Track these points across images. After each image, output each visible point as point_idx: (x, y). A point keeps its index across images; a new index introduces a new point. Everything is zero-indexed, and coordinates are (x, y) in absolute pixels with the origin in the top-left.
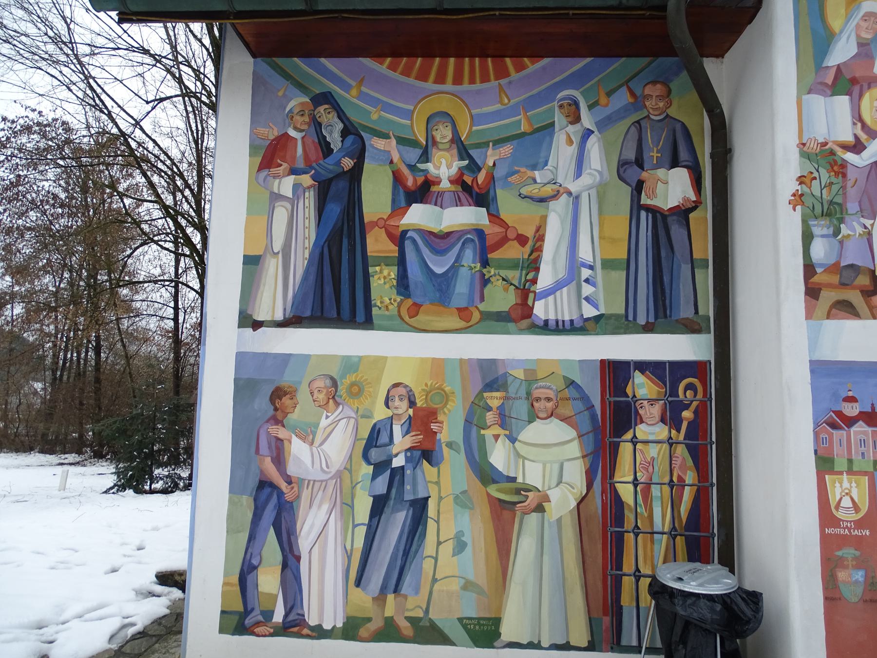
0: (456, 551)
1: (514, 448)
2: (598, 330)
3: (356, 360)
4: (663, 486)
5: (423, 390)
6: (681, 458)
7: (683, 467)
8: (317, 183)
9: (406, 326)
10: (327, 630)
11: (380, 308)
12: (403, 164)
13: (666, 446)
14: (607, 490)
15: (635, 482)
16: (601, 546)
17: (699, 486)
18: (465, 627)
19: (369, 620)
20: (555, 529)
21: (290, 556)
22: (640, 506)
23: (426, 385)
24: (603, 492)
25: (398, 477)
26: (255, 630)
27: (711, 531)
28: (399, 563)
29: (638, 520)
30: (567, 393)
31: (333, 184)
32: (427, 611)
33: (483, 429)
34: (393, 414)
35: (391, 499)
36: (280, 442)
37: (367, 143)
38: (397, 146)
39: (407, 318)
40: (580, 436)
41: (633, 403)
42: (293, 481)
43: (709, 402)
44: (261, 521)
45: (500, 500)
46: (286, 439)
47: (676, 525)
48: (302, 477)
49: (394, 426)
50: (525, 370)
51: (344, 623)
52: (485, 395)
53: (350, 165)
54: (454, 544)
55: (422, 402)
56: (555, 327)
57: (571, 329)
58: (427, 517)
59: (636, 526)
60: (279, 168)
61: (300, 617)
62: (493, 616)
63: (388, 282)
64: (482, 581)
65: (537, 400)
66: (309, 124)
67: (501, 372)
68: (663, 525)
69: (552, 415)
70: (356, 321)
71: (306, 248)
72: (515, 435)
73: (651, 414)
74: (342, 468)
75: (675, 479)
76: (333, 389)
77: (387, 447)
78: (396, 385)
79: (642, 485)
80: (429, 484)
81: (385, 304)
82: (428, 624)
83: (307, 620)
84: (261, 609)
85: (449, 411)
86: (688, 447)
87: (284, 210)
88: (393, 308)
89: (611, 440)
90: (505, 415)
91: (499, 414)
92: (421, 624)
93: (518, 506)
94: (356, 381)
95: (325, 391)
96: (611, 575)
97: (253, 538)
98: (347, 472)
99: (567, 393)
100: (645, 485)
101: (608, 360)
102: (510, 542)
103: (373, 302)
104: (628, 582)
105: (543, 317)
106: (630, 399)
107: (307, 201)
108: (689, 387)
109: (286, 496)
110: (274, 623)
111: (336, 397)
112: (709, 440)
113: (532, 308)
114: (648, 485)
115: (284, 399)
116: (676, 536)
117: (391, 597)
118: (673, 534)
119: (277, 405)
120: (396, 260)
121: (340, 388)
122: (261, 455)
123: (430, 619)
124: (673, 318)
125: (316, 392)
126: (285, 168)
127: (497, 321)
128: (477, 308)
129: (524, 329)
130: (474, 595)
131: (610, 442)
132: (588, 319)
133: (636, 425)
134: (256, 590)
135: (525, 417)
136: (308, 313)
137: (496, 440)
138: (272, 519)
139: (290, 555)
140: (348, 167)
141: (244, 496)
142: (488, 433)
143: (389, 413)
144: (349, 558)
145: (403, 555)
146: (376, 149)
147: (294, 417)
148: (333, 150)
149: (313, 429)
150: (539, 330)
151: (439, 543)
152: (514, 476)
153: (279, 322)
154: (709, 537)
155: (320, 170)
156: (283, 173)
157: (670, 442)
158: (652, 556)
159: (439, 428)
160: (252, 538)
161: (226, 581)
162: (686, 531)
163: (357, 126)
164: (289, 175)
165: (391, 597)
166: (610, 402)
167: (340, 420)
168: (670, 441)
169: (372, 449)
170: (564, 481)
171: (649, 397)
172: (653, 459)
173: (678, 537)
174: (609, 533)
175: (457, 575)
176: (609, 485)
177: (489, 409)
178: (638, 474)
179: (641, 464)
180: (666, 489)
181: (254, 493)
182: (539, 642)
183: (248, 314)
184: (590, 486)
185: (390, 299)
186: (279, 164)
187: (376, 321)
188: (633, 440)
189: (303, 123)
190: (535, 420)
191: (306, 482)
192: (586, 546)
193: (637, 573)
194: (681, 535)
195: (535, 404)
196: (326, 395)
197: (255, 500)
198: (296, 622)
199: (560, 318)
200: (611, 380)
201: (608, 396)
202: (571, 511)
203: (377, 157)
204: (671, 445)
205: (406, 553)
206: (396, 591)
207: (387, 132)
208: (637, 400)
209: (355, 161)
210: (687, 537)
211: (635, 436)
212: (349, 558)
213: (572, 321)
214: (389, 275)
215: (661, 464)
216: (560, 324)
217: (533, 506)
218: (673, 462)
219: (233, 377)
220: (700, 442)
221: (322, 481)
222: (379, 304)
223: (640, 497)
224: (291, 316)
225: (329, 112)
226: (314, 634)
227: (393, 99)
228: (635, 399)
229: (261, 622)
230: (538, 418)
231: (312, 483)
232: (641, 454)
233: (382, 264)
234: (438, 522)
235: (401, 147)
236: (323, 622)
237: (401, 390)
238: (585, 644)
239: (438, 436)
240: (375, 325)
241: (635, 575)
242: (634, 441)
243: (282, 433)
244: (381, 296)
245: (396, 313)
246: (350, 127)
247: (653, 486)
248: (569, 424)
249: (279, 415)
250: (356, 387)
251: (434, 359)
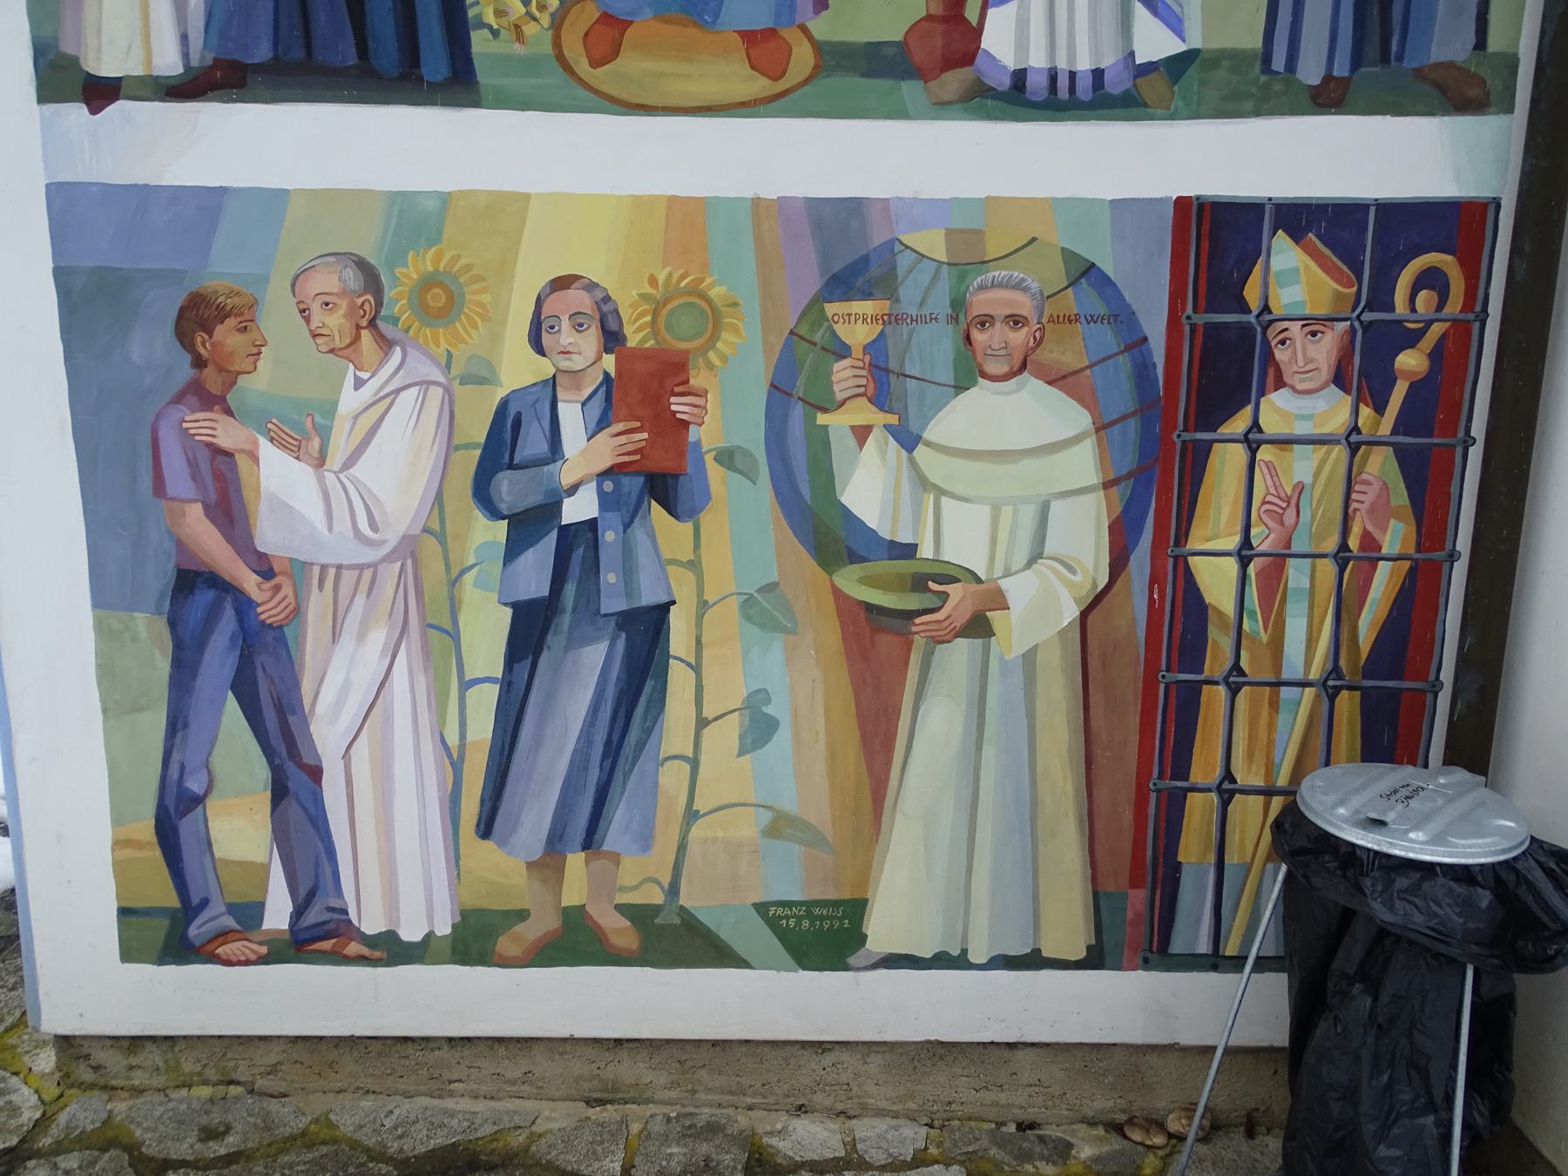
0: (749, 741)
1: (912, 462)
2: (1178, 102)
3: (432, 204)
4: (1318, 561)
5: (644, 297)
6: (1376, 486)
7: (1381, 511)
9: (581, 93)
10: (411, 944)
11: (495, 33)
13: (1339, 453)
14: (1165, 573)
15: (1244, 553)
16: (1138, 719)
17: (1416, 561)
18: (773, 923)
19: (522, 915)
20: (1018, 678)
21: (290, 767)
22: (1253, 614)
23: (653, 281)
24: (1155, 579)
25: (581, 551)
26: (219, 951)
27: (1432, 677)
28: (594, 775)
29: (1243, 653)
30: (1070, 302)
32: (673, 890)
33: (825, 410)
34: (558, 370)
35: (563, 611)
36: (225, 458)
39: (582, 66)
40: (1101, 427)
41: (1259, 329)
42: (276, 568)
43: (1477, 325)
44: (199, 679)
45: (869, 607)
46: (242, 451)
47: (1343, 663)
48: (302, 559)
49: (560, 405)
50: (950, 233)
51: (453, 926)
52: (831, 309)
54: (741, 724)
55: (641, 335)
56: (1046, 94)
57: (1094, 98)
58: (668, 655)
59: (1237, 668)
61: (336, 916)
62: (847, 896)
64: (820, 813)
65: (983, 324)
67: (877, 238)
68: (1308, 663)
69: (1023, 367)
70: (420, 79)
72: (914, 429)
73: (1308, 361)
74: (417, 530)
75: (1353, 543)
76: (369, 297)
77: (546, 468)
78: (562, 283)
79: (1262, 558)
80: (671, 569)
81: (513, 18)
82: (677, 921)
83: (355, 922)
84: (230, 900)
85: (724, 358)
86: (1402, 454)
88: (538, 32)
89: (1186, 436)
90: (887, 371)
91: (871, 365)
92: (657, 921)
93: (917, 621)
94: (436, 271)
95: (344, 304)
96: (1158, 791)
97: (179, 726)
98: (431, 543)
99: (1070, 302)
100: (1271, 558)
101: (1198, 198)
102: (893, 715)
103: (471, 13)
104: (1200, 808)
105: (1010, 62)
106: (1252, 318)
108: (1432, 279)
109: (259, 610)
110: (269, 931)
111: (380, 323)
112: (1461, 434)
113: (978, 32)
114: (1279, 559)
115: (220, 331)
116: (1337, 690)
117: (575, 861)
118: (1329, 689)
119: (202, 350)
121: (389, 294)
122: (171, 499)
123: (682, 907)
124: (1405, 65)
125: (316, 307)
127: (869, 74)
128: (804, 29)
129: (949, 103)
130: (797, 849)
131: (1184, 442)
132: (1150, 67)
133: (1262, 393)
134: (208, 855)
135: (947, 376)
136: (262, 52)
137: (861, 441)
138: (229, 672)
139: (291, 764)
141: (137, 615)
142: (837, 423)
143: (545, 368)
144: (457, 767)
145: (604, 757)
147: (257, 384)
149: (318, 419)
150: (996, 103)
151: (702, 723)
152: (910, 541)
154: (1424, 691)
157: (1354, 442)
158: (1270, 743)
159: (695, 411)
160: (176, 724)
161: (122, 837)
162: (1366, 676)
165: (575, 861)
166: (1193, 328)
167: (397, 391)
168: (1354, 438)
169: (500, 475)
170: (1048, 551)
171: (1308, 311)
172: (1300, 488)
173: (1345, 693)
174: (1162, 687)
175: (753, 800)
176: (1171, 561)
177: (842, 352)
178: (1253, 531)
179: (1264, 503)
180: (1328, 568)
181: (168, 602)
182: (964, 952)
184: (1118, 564)
187: (485, 77)
188: (1250, 436)
190: (974, 383)
191: (316, 570)
192: (1097, 722)
193: (1226, 785)
194: (1350, 688)
195: (977, 335)
196: (350, 314)
197: (173, 624)
198: (326, 927)
199: (1062, 64)
200: (1204, 262)
201: (1189, 310)
202: (1063, 633)
204: (1354, 449)
205: (613, 750)
206: (590, 842)
208: (1272, 322)
210: (1366, 694)
211: (1256, 425)
212: (457, 767)
213: (1098, 74)
215: (1319, 502)
216: (1063, 82)
217: (961, 619)
218: (1354, 496)
219: (50, 265)
220: (1436, 441)
221: (361, 568)
222: (490, 18)
223: (1252, 592)
224: (209, 62)
226: (377, 954)
228: (1267, 317)
229: (232, 931)
230: (984, 375)
231: (332, 572)
232: (1268, 477)
234: (697, 668)
236: (399, 927)
237: (576, 299)
238: (1080, 953)
239: (694, 433)
240: (482, 90)
241: (1219, 789)
242: (1253, 440)
243: (227, 434)
245: (547, 48)
247: (1291, 562)
248: (1072, 393)
249: (211, 377)
250: (438, 291)
251: (673, 200)
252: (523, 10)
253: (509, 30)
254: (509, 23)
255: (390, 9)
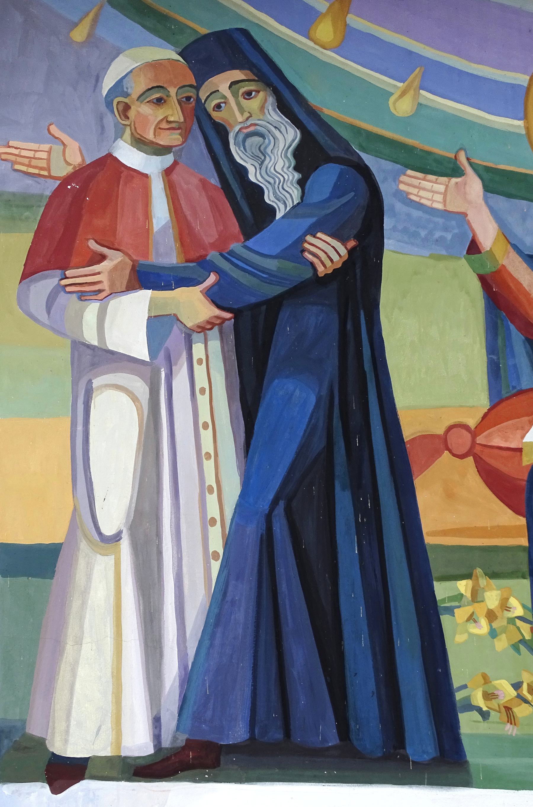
8: (228, 315)
11: (485, 715)
12: (513, 255)
31: (284, 314)
37: (385, 189)
38: (486, 202)
53: (336, 258)
60: (96, 268)
63: (504, 630)
66: (186, 133)
70: (405, 759)
71: (213, 522)
81: (503, 700)
87: (124, 398)
103: (459, 696)
107: (200, 371)
120: (524, 558)
126: (115, 268)
140: (328, 263)
146: (420, 206)
148: (272, 211)
153: (143, 762)
155: (236, 274)
156: (112, 284)
163: (344, 134)
164: (130, 288)
183: (32, 738)
185: (517, 686)
186: (95, 253)
189: (164, 125)
203: (423, 233)
207: (452, 156)
209: (352, 244)
214: (504, 606)
222: (479, 700)
225: (248, 94)
227: (459, 54)
233: (479, 571)
235: (501, 202)
240: (472, 769)
244: (485, 678)
246: (322, 138)
252: (513, 693)
253: (500, 712)
254: (499, 706)
255: (373, 693)
